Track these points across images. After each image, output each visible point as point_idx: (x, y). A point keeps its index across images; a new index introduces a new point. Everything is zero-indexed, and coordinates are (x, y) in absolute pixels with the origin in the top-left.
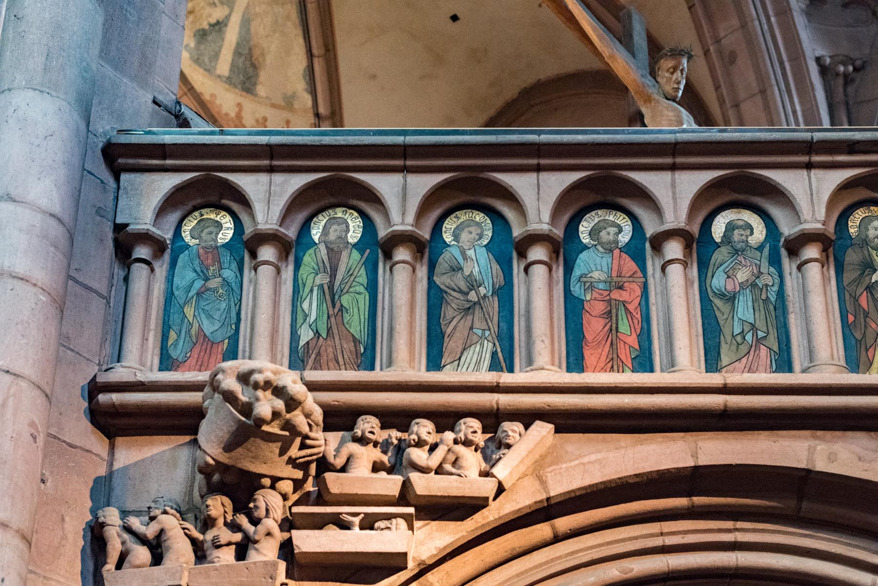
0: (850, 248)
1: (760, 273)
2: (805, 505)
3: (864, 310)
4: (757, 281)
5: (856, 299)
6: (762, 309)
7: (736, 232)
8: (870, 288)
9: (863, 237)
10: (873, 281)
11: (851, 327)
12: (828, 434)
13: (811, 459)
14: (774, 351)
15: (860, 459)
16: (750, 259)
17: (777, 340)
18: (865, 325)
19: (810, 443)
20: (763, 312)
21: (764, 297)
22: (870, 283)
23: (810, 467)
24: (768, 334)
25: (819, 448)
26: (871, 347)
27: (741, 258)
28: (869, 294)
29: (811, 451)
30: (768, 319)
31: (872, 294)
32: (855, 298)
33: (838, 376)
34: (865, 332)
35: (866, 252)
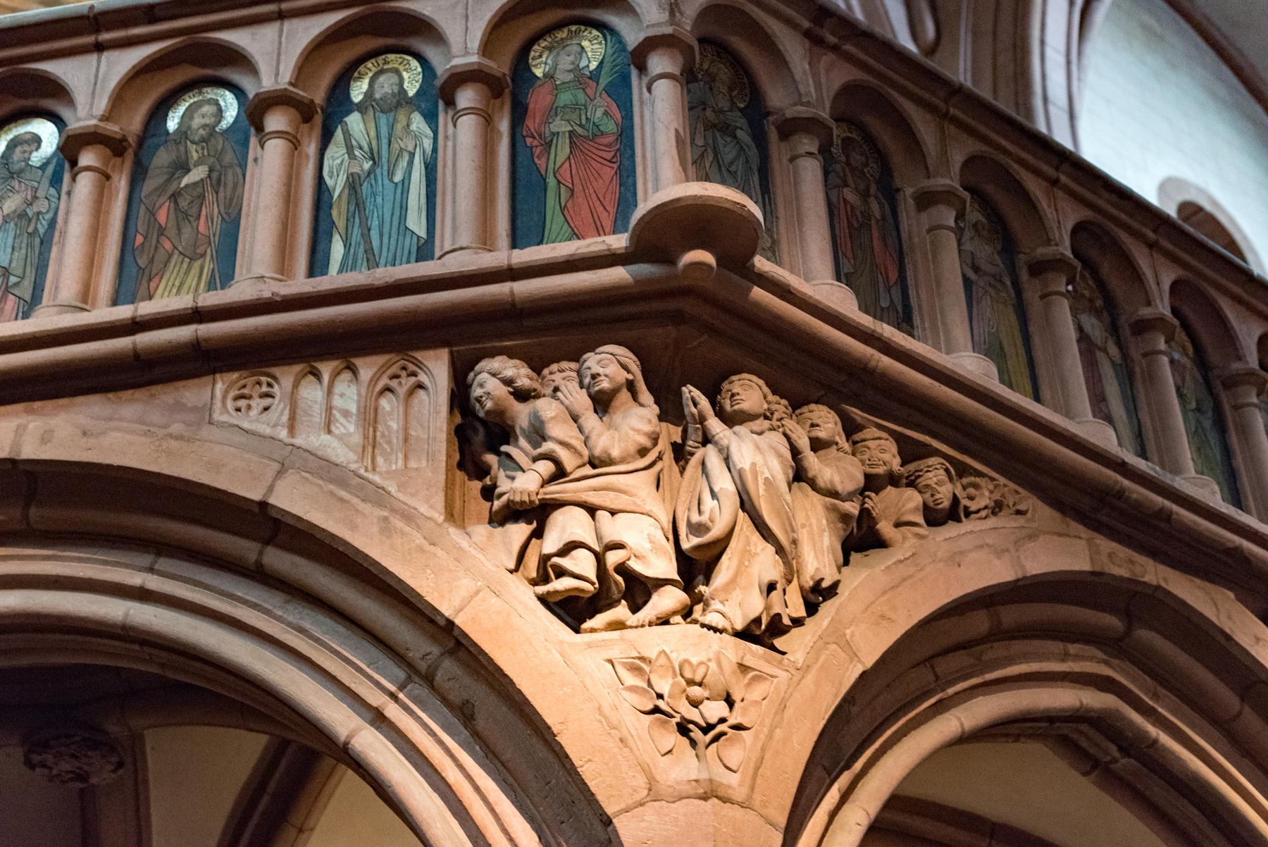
0: (162, 148)
1: (35, 198)
2: (34, 512)
3: (160, 225)
4: (28, 210)
5: (152, 214)
6: (24, 245)
7: (19, 149)
8: (174, 197)
9: (184, 130)
10: (182, 185)
11: (136, 252)
12: (49, 404)
13: (16, 444)
14: (24, 300)
15: (85, 434)
16: (26, 182)
17: (32, 284)
18: (156, 247)
19: (20, 421)
20: (24, 251)
21: (30, 230)
22: (178, 187)
23: (13, 456)
24: (23, 278)
25: (31, 426)
26: (157, 274)
27: (15, 183)
28: (172, 204)
29: (20, 430)
30: (29, 260)
31: (176, 203)
32: (151, 212)
33: (56, 318)
34: (153, 257)
35: (182, 149)
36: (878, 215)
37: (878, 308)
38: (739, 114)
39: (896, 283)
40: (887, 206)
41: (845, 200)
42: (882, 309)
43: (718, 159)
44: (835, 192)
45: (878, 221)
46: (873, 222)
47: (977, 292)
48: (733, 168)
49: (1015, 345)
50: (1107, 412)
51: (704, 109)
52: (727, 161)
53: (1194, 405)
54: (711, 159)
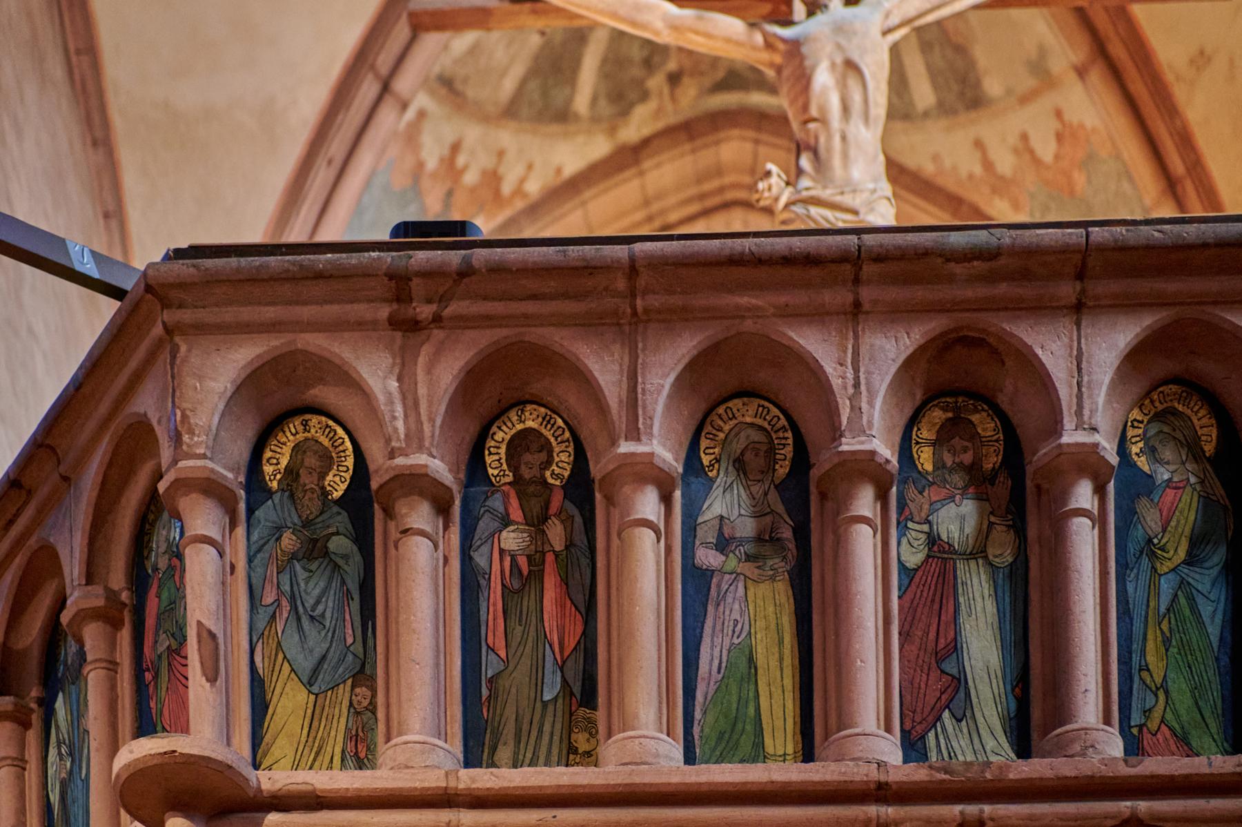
36: (558, 545)
37: (539, 705)
38: (336, 509)
39: (575, 648)
40: (578, 520)
41: (502, 551)
42: (545, 704)
43: (297, 613)
44: (485, 549)
45: (557, 554)
46: (550, 557)
47: (719, 586)
48: (320, 608)
49: (781, 642)
50: (954, 672)
51: (279, 539)
52: (310, 602)
53: (1182, 554)
54: (285, 615)
